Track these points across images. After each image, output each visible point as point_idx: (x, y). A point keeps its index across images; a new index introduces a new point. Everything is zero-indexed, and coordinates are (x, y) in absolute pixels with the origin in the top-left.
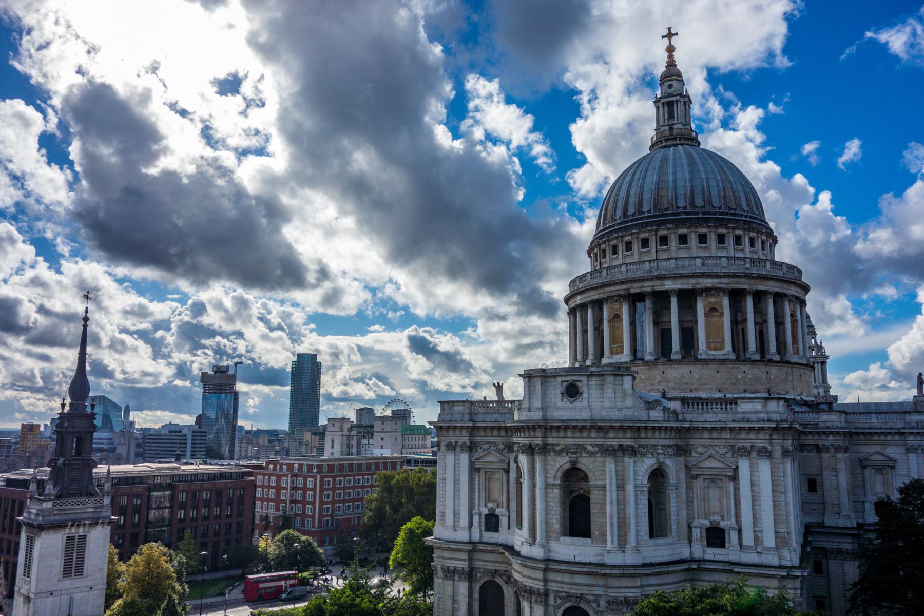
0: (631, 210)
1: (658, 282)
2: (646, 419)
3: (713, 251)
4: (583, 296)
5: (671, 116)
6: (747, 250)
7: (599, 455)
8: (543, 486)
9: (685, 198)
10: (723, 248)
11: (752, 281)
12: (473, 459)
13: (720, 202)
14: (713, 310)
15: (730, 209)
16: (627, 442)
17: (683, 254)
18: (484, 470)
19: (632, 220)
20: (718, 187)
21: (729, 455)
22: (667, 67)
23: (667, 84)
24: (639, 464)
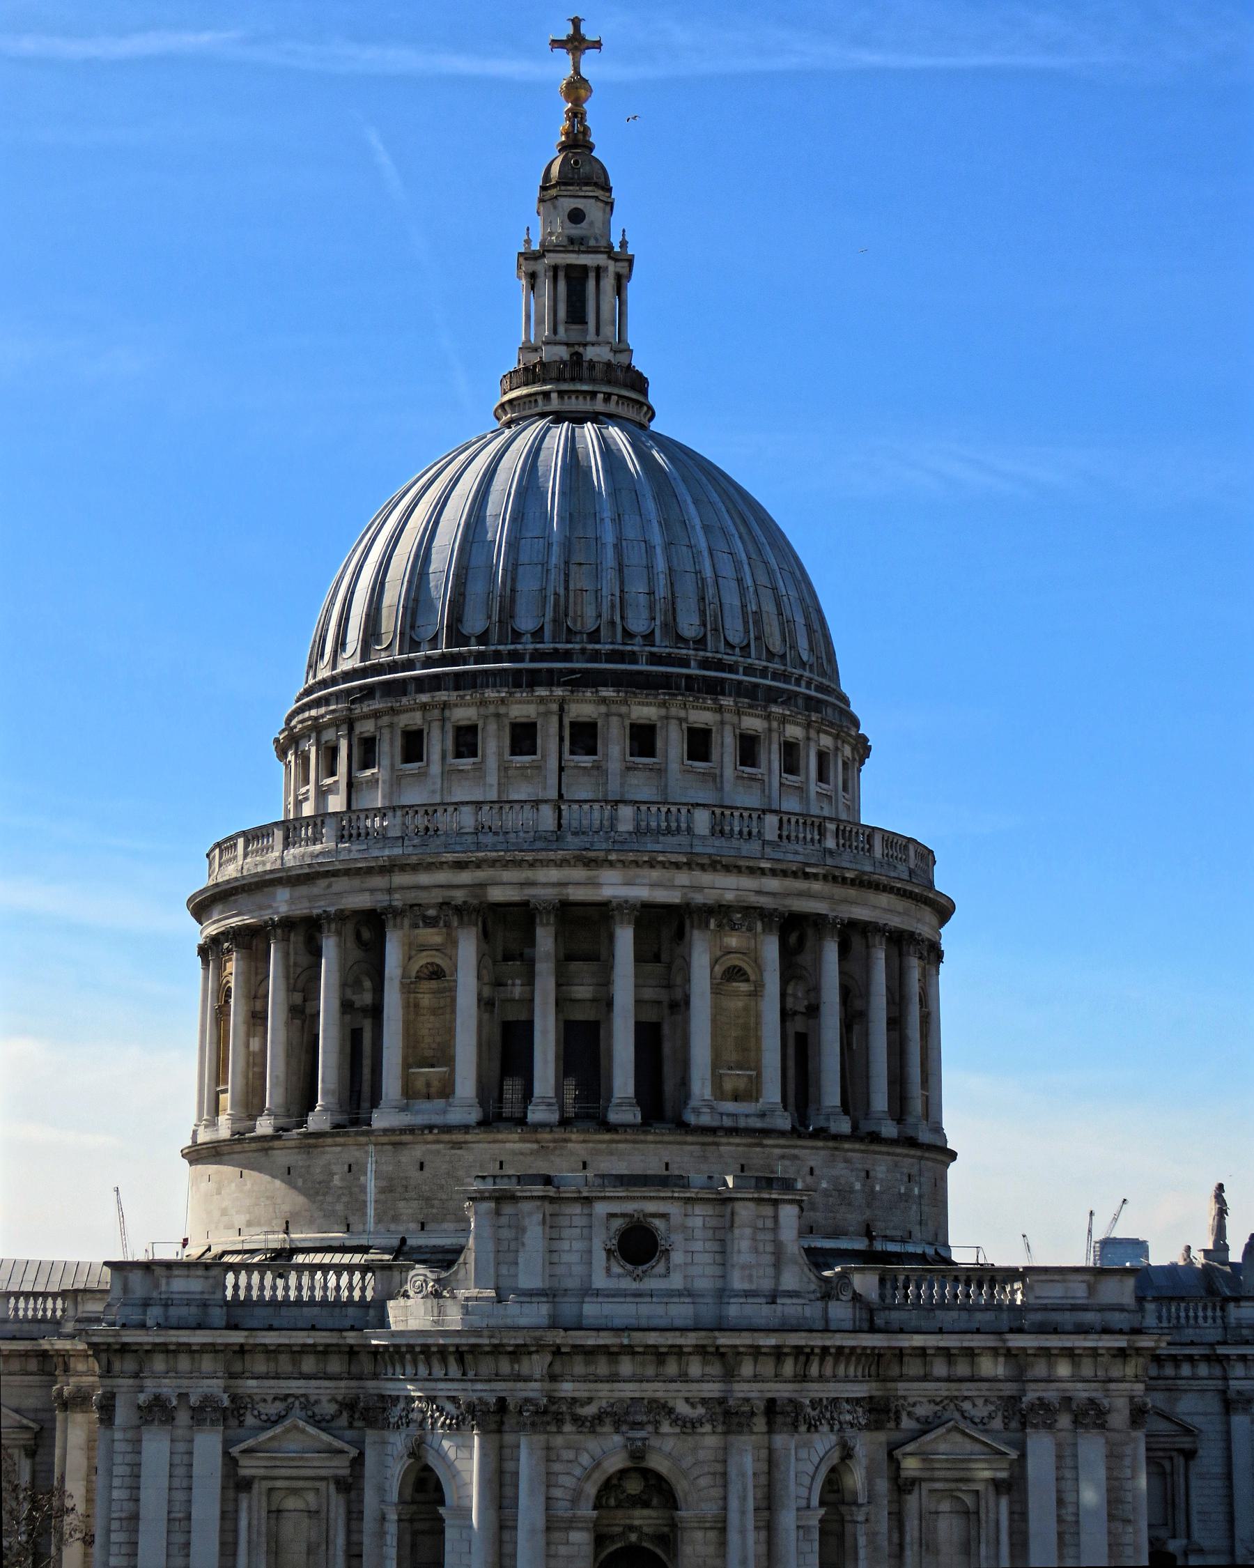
0: (475, 623)
1: (579, 874)
2: (819, 1325)
3: (728, 787)
4: (303, 890)
5: (576, 314)
6: (814, 787)
7: (707, 1428)
8: (541, 1523)
9: (651, 608)
10: (752, 778)
11: (839, 891)
12: (235, 1451)
13: (747, 631)
14: (735, 974)
15: (771, 656)
16: (783, 1391)
17: (641, 787)
18: (267, 1484)
19: (480, 658)
20: (740, 581)
21: (997, 1424)
22: (564, 147)
23: (568, 204)
24: (803, 1454)
